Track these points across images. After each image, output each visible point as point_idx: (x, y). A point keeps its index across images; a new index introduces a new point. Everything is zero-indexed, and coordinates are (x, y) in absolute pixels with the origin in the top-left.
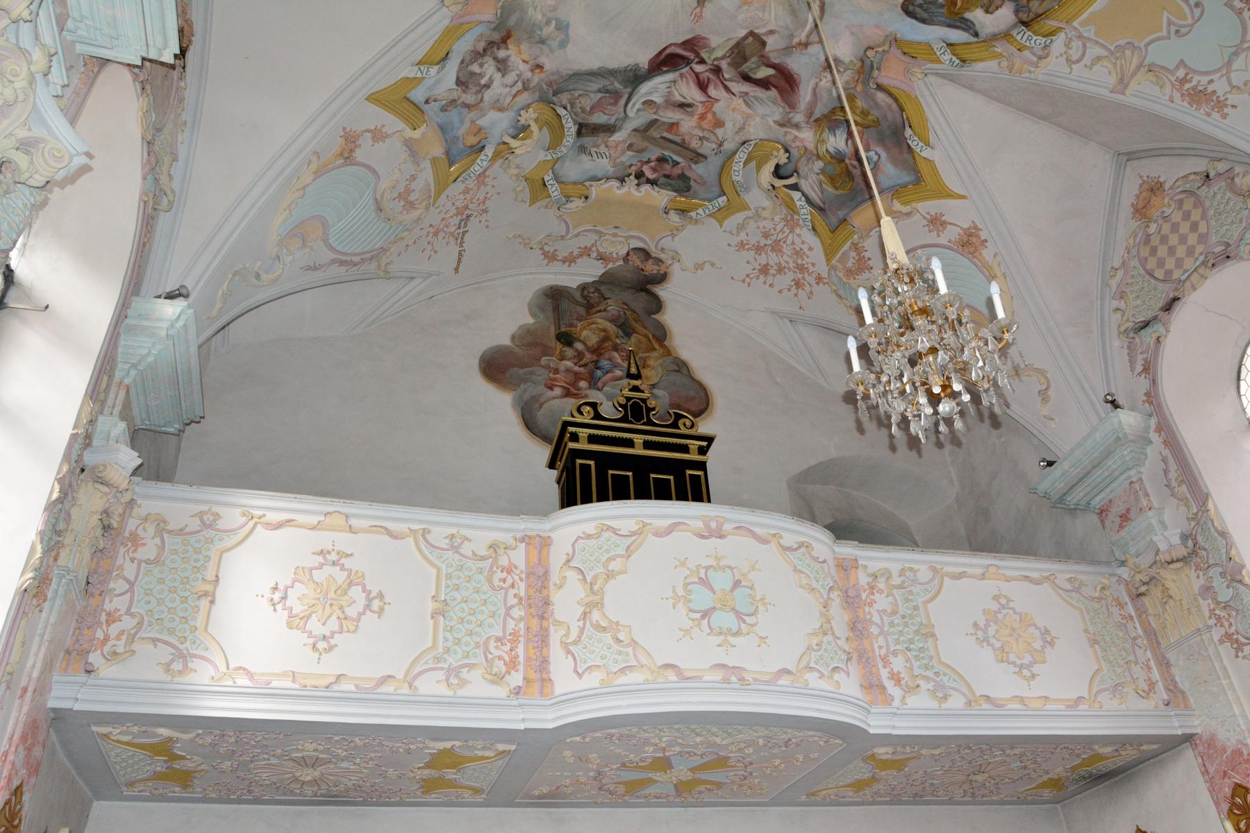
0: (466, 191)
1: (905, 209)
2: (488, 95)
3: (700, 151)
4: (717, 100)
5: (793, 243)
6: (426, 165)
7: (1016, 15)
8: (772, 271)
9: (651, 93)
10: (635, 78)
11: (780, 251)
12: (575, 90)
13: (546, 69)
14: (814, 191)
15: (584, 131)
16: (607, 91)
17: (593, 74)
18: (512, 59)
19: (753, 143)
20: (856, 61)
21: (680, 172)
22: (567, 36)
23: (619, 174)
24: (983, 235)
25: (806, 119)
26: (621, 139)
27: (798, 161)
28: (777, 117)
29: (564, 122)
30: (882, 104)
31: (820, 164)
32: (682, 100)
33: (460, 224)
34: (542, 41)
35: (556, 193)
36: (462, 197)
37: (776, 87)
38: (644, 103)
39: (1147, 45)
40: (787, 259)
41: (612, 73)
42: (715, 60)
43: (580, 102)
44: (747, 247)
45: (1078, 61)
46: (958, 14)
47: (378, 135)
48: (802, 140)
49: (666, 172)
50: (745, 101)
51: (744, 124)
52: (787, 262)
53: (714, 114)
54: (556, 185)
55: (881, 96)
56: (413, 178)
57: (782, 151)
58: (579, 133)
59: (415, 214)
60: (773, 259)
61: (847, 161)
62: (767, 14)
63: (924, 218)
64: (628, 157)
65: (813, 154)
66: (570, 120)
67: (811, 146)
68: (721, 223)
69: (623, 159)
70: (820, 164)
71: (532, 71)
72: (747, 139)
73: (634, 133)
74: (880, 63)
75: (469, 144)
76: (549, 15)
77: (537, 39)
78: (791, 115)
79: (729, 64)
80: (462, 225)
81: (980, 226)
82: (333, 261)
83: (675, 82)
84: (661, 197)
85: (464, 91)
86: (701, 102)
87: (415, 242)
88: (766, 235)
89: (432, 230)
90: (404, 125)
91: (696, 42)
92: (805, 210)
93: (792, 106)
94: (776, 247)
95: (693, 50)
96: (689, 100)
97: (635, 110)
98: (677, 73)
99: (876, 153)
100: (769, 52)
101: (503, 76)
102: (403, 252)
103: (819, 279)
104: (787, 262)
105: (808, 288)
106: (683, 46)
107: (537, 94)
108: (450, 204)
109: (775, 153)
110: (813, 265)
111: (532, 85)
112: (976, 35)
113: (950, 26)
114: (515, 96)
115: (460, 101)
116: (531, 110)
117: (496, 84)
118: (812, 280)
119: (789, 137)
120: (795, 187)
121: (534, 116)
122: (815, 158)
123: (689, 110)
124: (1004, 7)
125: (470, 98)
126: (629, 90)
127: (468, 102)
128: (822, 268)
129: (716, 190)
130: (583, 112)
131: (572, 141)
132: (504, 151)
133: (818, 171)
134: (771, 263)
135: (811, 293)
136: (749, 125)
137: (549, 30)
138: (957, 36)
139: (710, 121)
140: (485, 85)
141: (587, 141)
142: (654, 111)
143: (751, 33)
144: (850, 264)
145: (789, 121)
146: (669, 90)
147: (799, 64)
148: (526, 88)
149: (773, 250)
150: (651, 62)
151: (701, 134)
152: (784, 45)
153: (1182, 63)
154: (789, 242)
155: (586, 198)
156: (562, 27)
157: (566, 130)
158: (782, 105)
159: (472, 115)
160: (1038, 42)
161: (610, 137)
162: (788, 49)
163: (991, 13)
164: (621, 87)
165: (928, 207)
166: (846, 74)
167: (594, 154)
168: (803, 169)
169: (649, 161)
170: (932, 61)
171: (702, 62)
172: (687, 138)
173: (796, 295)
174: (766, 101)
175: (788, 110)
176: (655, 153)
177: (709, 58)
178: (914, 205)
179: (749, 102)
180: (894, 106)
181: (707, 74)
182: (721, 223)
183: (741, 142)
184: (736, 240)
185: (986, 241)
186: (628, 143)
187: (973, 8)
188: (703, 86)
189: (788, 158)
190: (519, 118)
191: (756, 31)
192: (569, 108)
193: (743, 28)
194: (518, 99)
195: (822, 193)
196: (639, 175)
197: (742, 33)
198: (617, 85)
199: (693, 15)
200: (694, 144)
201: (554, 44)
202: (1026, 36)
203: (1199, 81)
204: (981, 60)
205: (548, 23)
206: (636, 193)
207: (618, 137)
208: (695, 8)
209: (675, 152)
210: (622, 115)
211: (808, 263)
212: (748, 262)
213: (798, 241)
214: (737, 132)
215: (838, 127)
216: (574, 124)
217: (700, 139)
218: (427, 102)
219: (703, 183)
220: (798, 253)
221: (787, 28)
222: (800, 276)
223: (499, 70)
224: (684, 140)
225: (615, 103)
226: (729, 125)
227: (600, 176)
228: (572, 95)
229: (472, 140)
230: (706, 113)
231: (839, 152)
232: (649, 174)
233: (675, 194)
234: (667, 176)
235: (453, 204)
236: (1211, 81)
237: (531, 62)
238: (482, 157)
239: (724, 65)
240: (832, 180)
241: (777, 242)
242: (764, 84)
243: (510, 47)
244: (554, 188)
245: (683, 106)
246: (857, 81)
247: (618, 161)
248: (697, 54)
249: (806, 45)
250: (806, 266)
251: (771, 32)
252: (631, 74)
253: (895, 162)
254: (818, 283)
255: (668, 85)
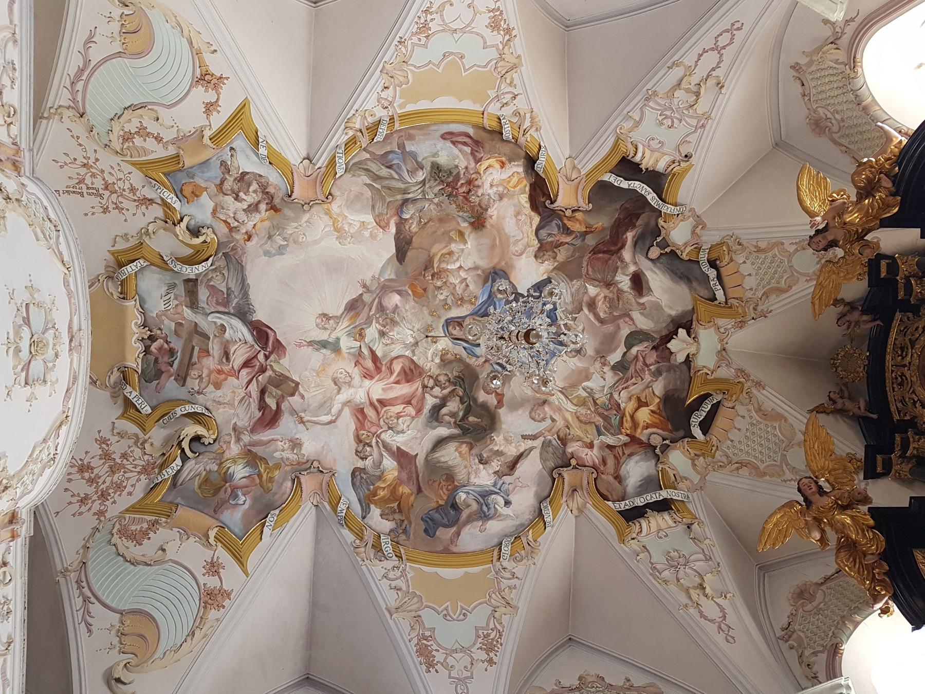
0: (133, 190)
1: (212, 540)
2: (229, 199)
3: (188, 379)
4: (238, 378)
5: (128, 479)
6: (172, 151)
7: (390, 532)
8: (86, 475)
9: (232, 328)
10: (243, 314)
11: (113, 472)
12: (228, 270)
13: (247, 243)
14: (188, 475)
15: (191, 283)
16: (228, 295)
17: (244, 280)
18: (258, 216)
19: (210, 415)
20: (305, 458)
21: (163, 370)
22: (274, 255)
23: (150, 322)
24: (226, 603)
25: (247, 443)
26: (185, 315)
27: (209, 452)
28: (240, 424)
29: (203, 264)
30: (283, 488)
31: (215, 468)
32: (232, 352)
33: (93, 188)
34: (270, 237)
35: (130, 270)
36: (127, 186)
37: (263, 414)
38: (222, 326)
39: (427, 607)
40: (106, 481)
41: (245, 295)
42: (271, 366)
43: (217, 276)
44: (104, 446)
45: (390, 579)
46: (370, 501)
47: (210, 108)
48: (229, 448)
49: (160, 360)
50: (244, 397)
51: (224, 403)
52: (104, 482)
53: (226, 379)
54: (137, 270)
55: (289, 484)
56: (158, 139)
57: (214, 437)
58: (188, 281)
59: (116, 145)
60: (101, 469)
61: (228, 484)
62: (314, 389)
63: (213, 558)
64: (169, 325)
65: (221, 460)
66: (204, 269)
67: (227, 455)
68: (122, 416)
69: (166, 322)
70: (215, 468)
71: (247, 233)
72: (212, 411)
73: (194, 324)
74: (310, 472)
75: (183, 188)
76: (291, 239)
77: (272, 233)
78: (246, 432)
79: (270, 376)
80: (91, 191)
81: (232, 597)
82: (87, 62)
83: (246, 343)
84: (134, 359)
85: (235, 179)
86: (233, 367)
87: (80, 145)
88: (124, 456)
89: (91, 162)
90: (214, 130)
91: (281, 348)
92: (169, 472)
93: (252, 431)
94: (113, 470)
95: (274, 348)
96: (232, 358)
97: (214, 320)
98: (253, 343)
99: (245, 501)
100: (288, 400)
101: (244, 210)
102: (71, 134)
103: (101, 513)
104: (104, 482)
105: (84, 509)
106: (275, 341)
107: (225, 240)
108: (121, 175)
109: (211, 432)
110: (114, 502)
111: (234, 234)
112: (364, 518)
113: (359, 500)
114: (225, 222)
115: (228, 177)
116: (213, 236)
117: (238, 204)
118: (96, 507)
119: (227, 438)
120: (185, 458)
121: (208, 240)
122: (218, 462)
123: (224, 360)
124: (390, 522)
125: (229, 184)
126: (232, 311)
127: (225, 183)
128: (113, 510)
129: (155, 402)
130: (208, 280)
131: (187, 273)
132: (171, 220)
133: (208, 469)
134: (96, 471)
135: (81, 514)
136: (225, 407)
137: (279, 240)
138: (357, 508)
139: (218, 378)
140: (238, 196)
141: (181, 289)
142: (217, 335)
143: (297, 384)
144: (133, 528)
145: (240, 433)
146: (238, 341)
147: (287, 423)
148: (231, 229)
149: (111, 467)
150: (259, 322)
151: (204, 376)
152: (296, 409)
153: (433, 630)
154: (127, 475)
155: (124, 298)
156: (281, 250)
157: (197, 266)
158: (251, 424)
159: (213, 189)
160: (388, 549)
161: (186, 306)
162: (294, 412)
163: (382, 518)
164: (234, 305)
165: (223, 555)
166: (294, 455)
167: (167, 297)
168: (204, 459)
169: (167, 342)
170: (330, 503)
171: (267, 357)
172: (198, 366)
173: (70, 503)
174: (250, 412)
175: (248, 429)
176: (177, 344)
177: (271, 361)
178: (219, 544)
179: (244, 400)
180: (286, 496)
181: (258, 364)
182: (122, 416)
183: (207, 406)
184: (106, 434)
185: (224, 607)
186: (184, 322)
187: (378, 507)
188: (247, 364)
189: (210, 443)
190: (206, 228)
191: (300, 386)
192: (211, 268)
193: (300, 377)
194: (222, 225)
195: (189, 480)
196: (152, 338)
197: (295, 378)
198: (236, 301)
199: (300, 341)
200: (194, 373)
201: (267, 247)
202: (387, 540)
203: (432, 645)
204: (350, 529)
205: (285, 239)
206: (134, 339)
207: (188, 313)
208: (305, 341)
209: (182, 360)
210: (209, 312)
211: (113, 497)
212: (87, 453)
213: (133, 481)
214: (215, 401)
215: (252, 467)
216: (196, 275)
217: (199, 376)
218: (232, 149)
219: (158, 390)
220: (119, 487)
221: (309, 406)
222: (95, 497)
223: (250, 206)
224: (195, 364)
225: (218, 303)
226: (219, 393)
227: (146, 306)
228: (224, 268)
229: (187, 191)
230: (224, 373)
231: (232, 476)
232: (154, 347)
233: (140, 372)
234: (156, 360)
235: (120, 179)
236: (436, 650)
237: (254, 231)
238: (175, 198)
239: (269, 373)
240: (206, 481)
241: (122, 466)
242: (263, 406)
243: (268, 213)
244: (134, 268)
245: (227, 355)
246: (292, 464)
247: (164, 318)
248: (271, 353)
249: (302, 422)
250: (109, 498)
251: (303, 397)
252: (246, 309)
253: (245, 515)
254: (95, 514)
255: (242, 338)
